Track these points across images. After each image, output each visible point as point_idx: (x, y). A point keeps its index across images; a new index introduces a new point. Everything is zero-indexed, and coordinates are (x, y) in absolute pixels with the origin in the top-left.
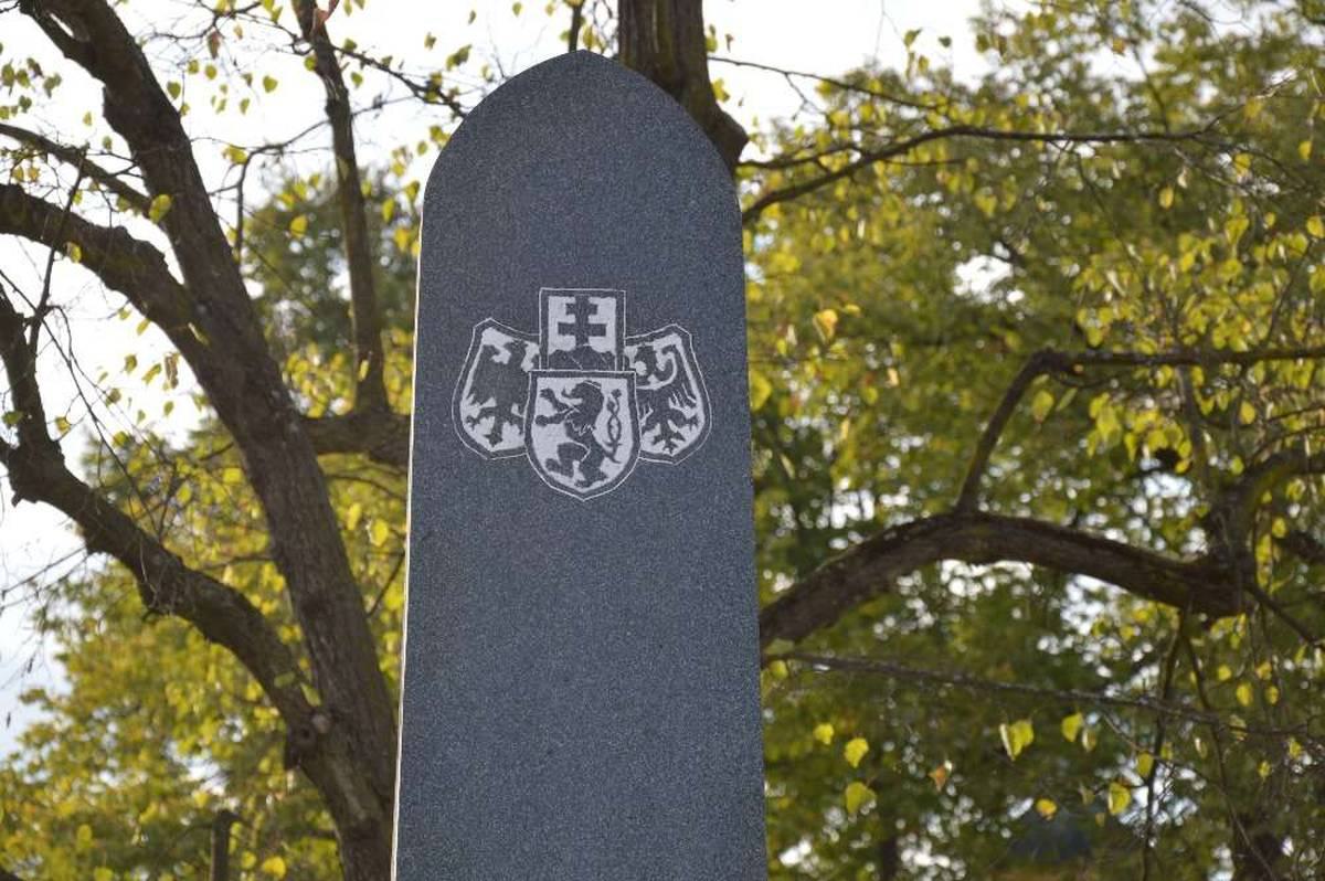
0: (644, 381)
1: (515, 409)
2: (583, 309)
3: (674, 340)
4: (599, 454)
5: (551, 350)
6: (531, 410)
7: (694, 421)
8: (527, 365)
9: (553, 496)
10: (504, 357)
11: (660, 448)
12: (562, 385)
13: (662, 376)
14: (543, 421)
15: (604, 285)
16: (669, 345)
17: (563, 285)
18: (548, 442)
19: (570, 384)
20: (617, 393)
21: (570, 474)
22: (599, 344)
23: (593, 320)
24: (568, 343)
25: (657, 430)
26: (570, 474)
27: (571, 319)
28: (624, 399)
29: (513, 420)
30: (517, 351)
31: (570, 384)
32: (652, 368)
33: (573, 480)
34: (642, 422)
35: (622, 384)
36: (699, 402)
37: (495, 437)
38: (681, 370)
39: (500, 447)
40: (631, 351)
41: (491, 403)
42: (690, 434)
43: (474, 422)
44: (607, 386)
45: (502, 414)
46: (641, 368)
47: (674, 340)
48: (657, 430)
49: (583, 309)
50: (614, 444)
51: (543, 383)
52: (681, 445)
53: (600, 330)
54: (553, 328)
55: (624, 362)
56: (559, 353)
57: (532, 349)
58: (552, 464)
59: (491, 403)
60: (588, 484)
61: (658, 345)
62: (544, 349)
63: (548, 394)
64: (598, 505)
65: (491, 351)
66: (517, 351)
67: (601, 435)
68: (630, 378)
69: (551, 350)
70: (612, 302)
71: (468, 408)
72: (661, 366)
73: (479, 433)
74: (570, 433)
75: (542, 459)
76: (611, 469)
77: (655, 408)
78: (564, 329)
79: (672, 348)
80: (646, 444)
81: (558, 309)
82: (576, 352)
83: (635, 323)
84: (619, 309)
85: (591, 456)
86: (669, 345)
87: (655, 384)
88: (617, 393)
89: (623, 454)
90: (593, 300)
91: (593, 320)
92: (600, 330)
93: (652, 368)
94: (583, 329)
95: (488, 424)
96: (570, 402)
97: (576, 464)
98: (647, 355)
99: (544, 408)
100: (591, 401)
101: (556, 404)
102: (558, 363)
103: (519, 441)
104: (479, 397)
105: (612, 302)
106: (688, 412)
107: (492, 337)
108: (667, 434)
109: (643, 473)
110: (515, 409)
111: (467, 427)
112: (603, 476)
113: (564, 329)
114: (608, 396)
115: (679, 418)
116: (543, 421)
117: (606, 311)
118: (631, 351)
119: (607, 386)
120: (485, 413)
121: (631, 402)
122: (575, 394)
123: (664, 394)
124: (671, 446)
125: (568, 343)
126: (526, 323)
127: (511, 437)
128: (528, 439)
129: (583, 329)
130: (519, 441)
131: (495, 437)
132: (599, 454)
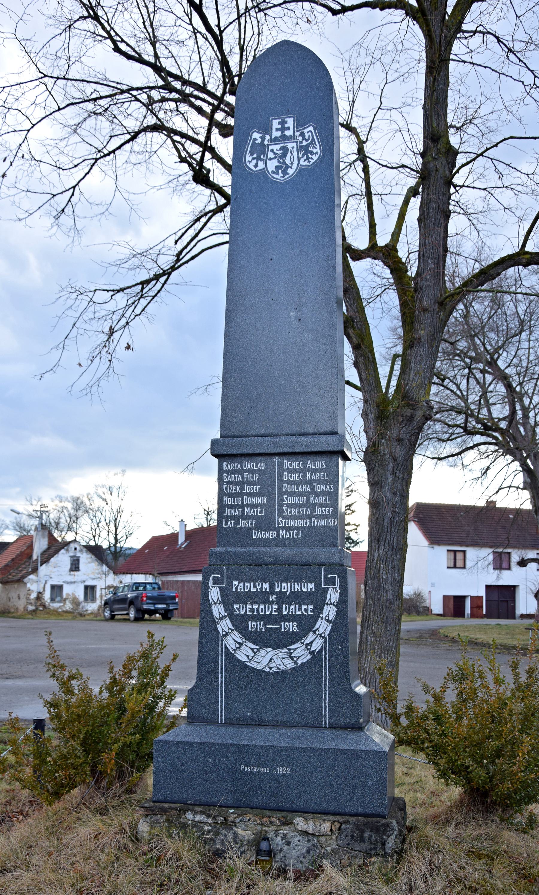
0: (301, 142)
1: (262, 157)
2: (283, 123)
3: (311, 128)
4: (287, 167)
5: (273, 137)
6: (267, 156)
7: (317, 153)
8: (266, 143)
9: (274, 182)
10: (259, 141)
11: (306, 163)
12: (276, 147)
13: (307, 140)
14: (270, 159)
15: (289, 113)
16: (309, 131)
17: (276, 115)
18: (272, 165)
19: (279, 147)
20: (293, 148)
21: (278, 174)
22: (288, 133)
23: (286, 126)
24: (279, 134)
25: (305, 157)
26: (278, 174)
27: (280, 126)
28: (295, 149)
29: (261, 160)
30: (263, 139)
31: (279, 147)
32: (304, 138)
33: (279, 177)
34: (301, 156)
35: (294, 145)
36: (318, 147)
37: (256, 166)
38: (313, 137)
39: (258, 169)
40: (297, 134)
41: (255, 156)
42: (315, 157)
43: (250, 162)
44: (290, 146)
45: (258, 159)
46: (300, 139)
47: (311, 128)
48: (305, 157)
49: (283, 123)
50: (292, 163)
51: (271, 147)
52: (312, 161)
53: (288, 128)
54: (274, 130)
55: (295, 137)
56: (276, 137)
57: (267, 137)
58: (273, 172)
59: (255, 156)
60: (283, 177)
61: (306, 131)
62: (271, 137)
63: (272, 151)
64: (286, 183)
65: (255, 139)
66: (263, 139)
67: (288, 161)
68: (297, 142)
69: (273, 137)
70: (292, 119)
71: (248, 158)
72: (307, 137)
73: (251, 166)
74: (279, 162)
75: (270, 171)
76: (291, 171)
77: (305, 150)
78: (277, 130)
79: (310, 131)
80: (302, 162)
81: (276, 124)
82: (281, 137)
83: (300, 125)
84: (294, 121)
85: (283, 167)
86: (309, 131)
87: (305, 143)
88: (293, 148)
89: (295, 166)
90: (286, 119)
91: (286, 126)
92: (288, 128)
93: (304, 138)
94: (283, 129)
95: (254, 162)
96: (278, 152)
97: (280, 171)
98: (302, 135)
99: (271, 155)
100: (285, 150)
101: (275, 154)
102: (275, 140)
103: (263, 166)
104: (252, 154)
105: (292, 119)
106: (315, 151)
107: (256, 136)
108: (308, 158)
109: (301, 171)
110: (262, 157)
111: (248, 164)
112: (288, 174)
113: (277, 130)
114: (290, 149)
115: (312, 153)
116: (270, 159)
117: (290, 122)
118: (297, 134)
119: (290, 146)
120: (253, 159)
121: (297, 150)
122: (280, 149)
123: (308, 145)
124: (309, 162)
125: (279, 134)
126: (265, 130)
127: (261, 165)
128: (266, 165)
129: (283, 129)
130: (263, 166)
131: (256, 166)
132: (287, 167)
